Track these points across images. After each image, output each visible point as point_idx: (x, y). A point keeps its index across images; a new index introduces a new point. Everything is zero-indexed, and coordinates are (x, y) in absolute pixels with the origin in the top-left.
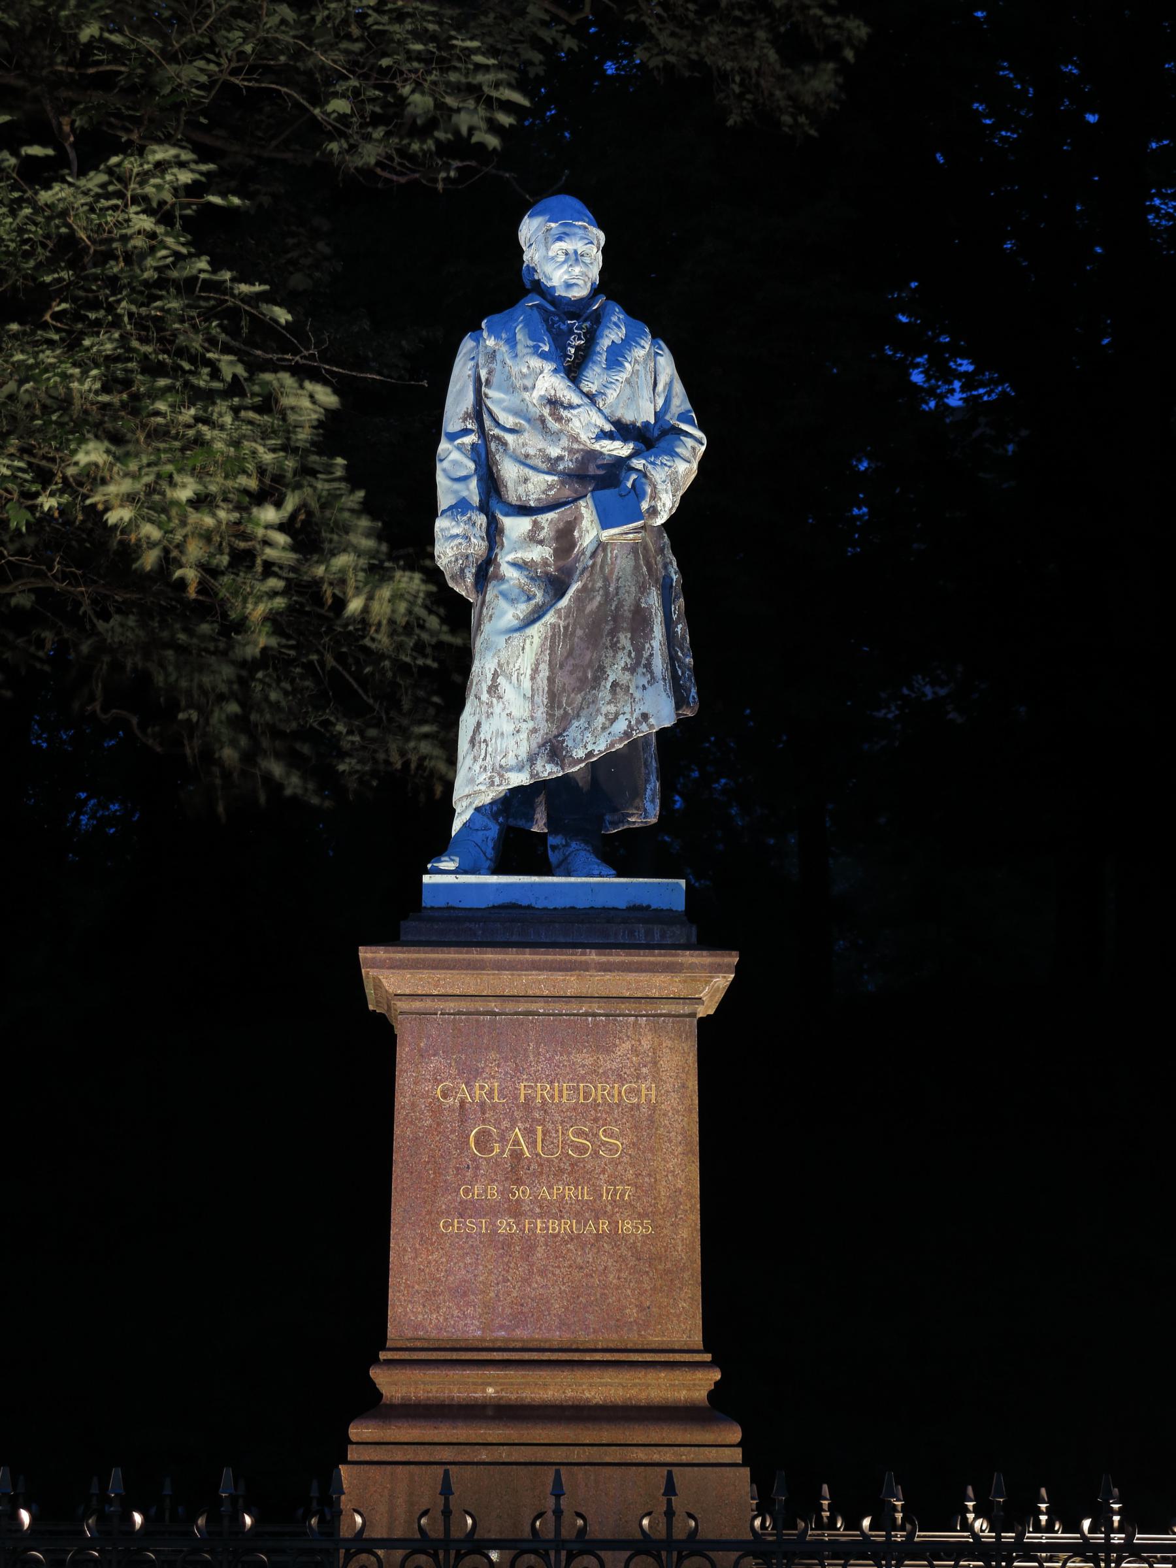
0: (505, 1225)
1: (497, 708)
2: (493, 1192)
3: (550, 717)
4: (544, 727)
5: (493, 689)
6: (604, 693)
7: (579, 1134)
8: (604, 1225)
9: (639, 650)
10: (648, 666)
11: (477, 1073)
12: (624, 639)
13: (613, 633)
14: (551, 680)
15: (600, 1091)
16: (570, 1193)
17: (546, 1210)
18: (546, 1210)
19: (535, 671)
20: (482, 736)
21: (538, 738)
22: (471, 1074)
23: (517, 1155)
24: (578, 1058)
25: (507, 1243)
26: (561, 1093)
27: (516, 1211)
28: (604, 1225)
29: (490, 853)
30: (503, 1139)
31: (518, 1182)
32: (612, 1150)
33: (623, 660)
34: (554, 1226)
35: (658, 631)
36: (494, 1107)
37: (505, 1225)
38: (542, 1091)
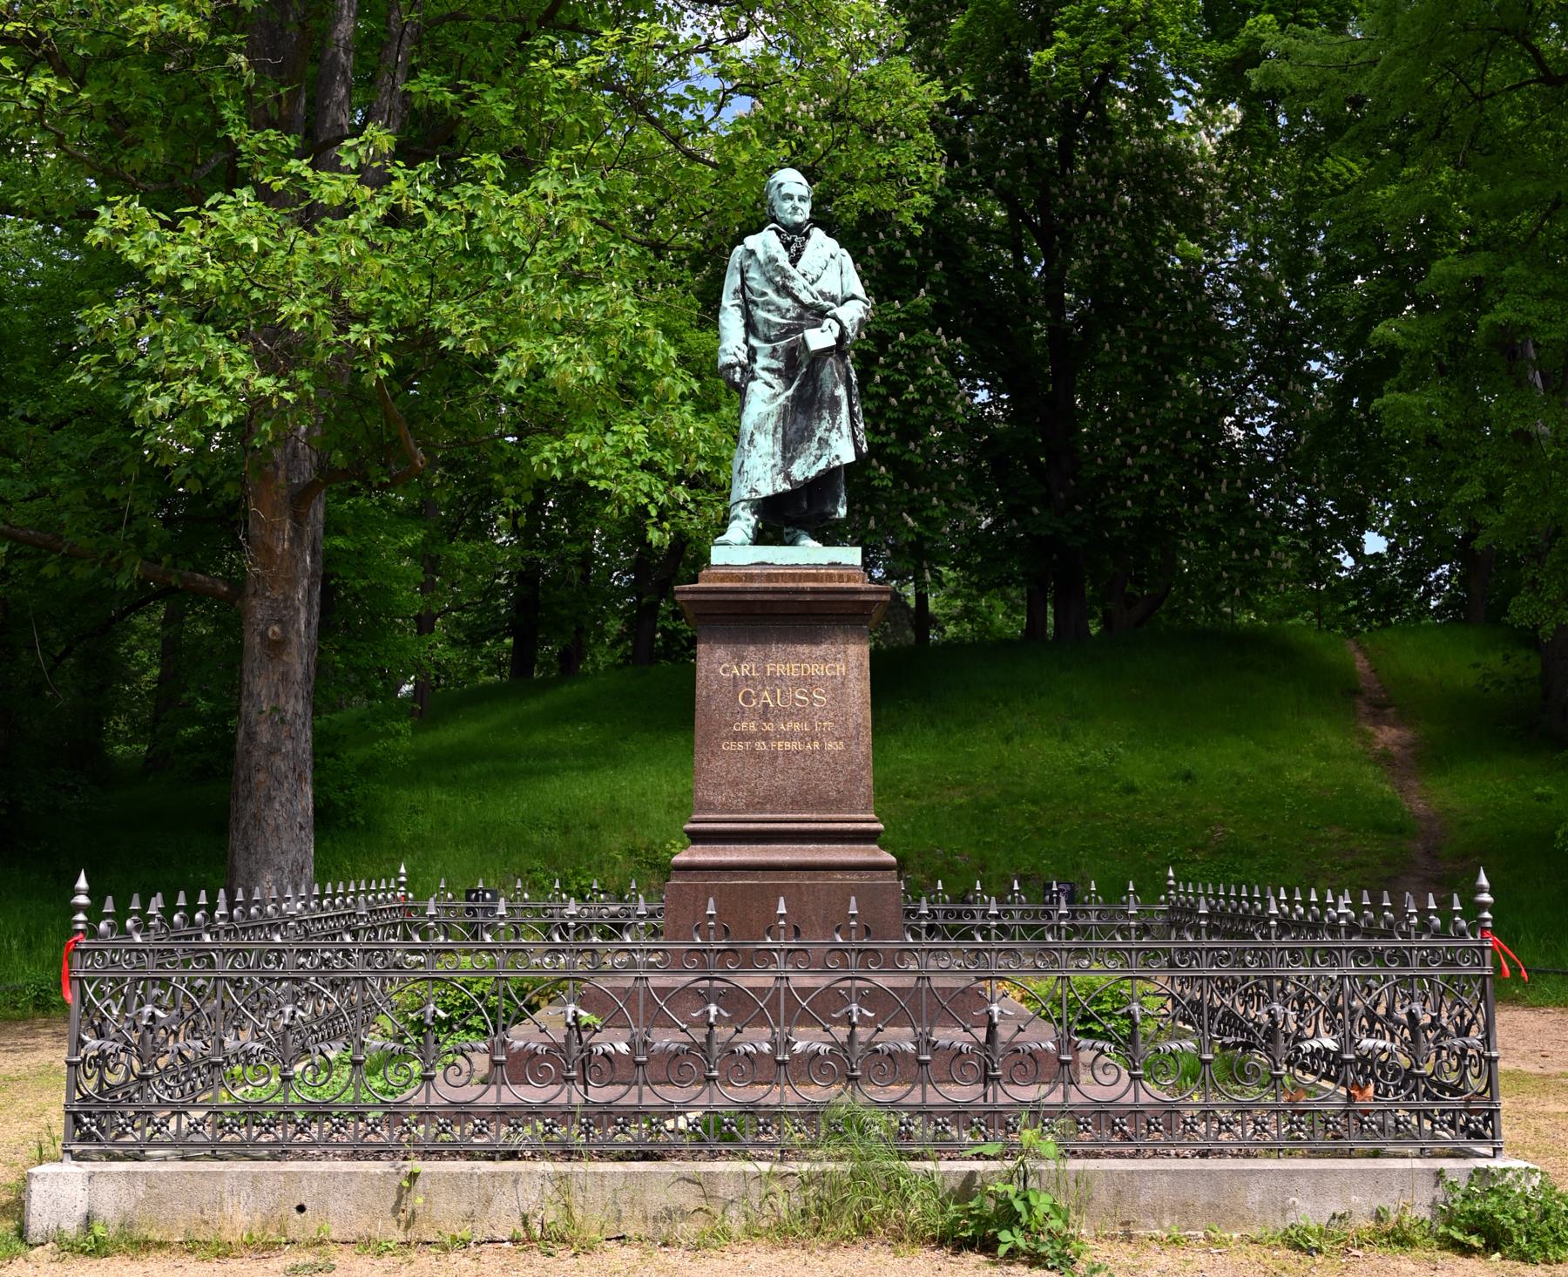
0: (760, 746)
1: (754, 452)
2: (753, 727)
3: (784, 458)
4: (780, 463)
5: (751, 442)
6: (815, 444)
7: (801, 693)
8: (816, 745)
9: (834, 419)
11: (742, 659)
12: (826, 414)
13: (819, 410)
15: (815, 669)
16: (797, 726)
17: (785, 737)
18: (785, 737)
19: (775, 431)
20: (745, 468)
21: (776, 470)
23: (766, 705)
25: (760, 756)
27: (766, 737)
28: (816, 745)
30: (758, 696)
31: (767, 720)
33: (825, 424)
34: (788, 745)
36: (753, 678)
37: (760, 746)
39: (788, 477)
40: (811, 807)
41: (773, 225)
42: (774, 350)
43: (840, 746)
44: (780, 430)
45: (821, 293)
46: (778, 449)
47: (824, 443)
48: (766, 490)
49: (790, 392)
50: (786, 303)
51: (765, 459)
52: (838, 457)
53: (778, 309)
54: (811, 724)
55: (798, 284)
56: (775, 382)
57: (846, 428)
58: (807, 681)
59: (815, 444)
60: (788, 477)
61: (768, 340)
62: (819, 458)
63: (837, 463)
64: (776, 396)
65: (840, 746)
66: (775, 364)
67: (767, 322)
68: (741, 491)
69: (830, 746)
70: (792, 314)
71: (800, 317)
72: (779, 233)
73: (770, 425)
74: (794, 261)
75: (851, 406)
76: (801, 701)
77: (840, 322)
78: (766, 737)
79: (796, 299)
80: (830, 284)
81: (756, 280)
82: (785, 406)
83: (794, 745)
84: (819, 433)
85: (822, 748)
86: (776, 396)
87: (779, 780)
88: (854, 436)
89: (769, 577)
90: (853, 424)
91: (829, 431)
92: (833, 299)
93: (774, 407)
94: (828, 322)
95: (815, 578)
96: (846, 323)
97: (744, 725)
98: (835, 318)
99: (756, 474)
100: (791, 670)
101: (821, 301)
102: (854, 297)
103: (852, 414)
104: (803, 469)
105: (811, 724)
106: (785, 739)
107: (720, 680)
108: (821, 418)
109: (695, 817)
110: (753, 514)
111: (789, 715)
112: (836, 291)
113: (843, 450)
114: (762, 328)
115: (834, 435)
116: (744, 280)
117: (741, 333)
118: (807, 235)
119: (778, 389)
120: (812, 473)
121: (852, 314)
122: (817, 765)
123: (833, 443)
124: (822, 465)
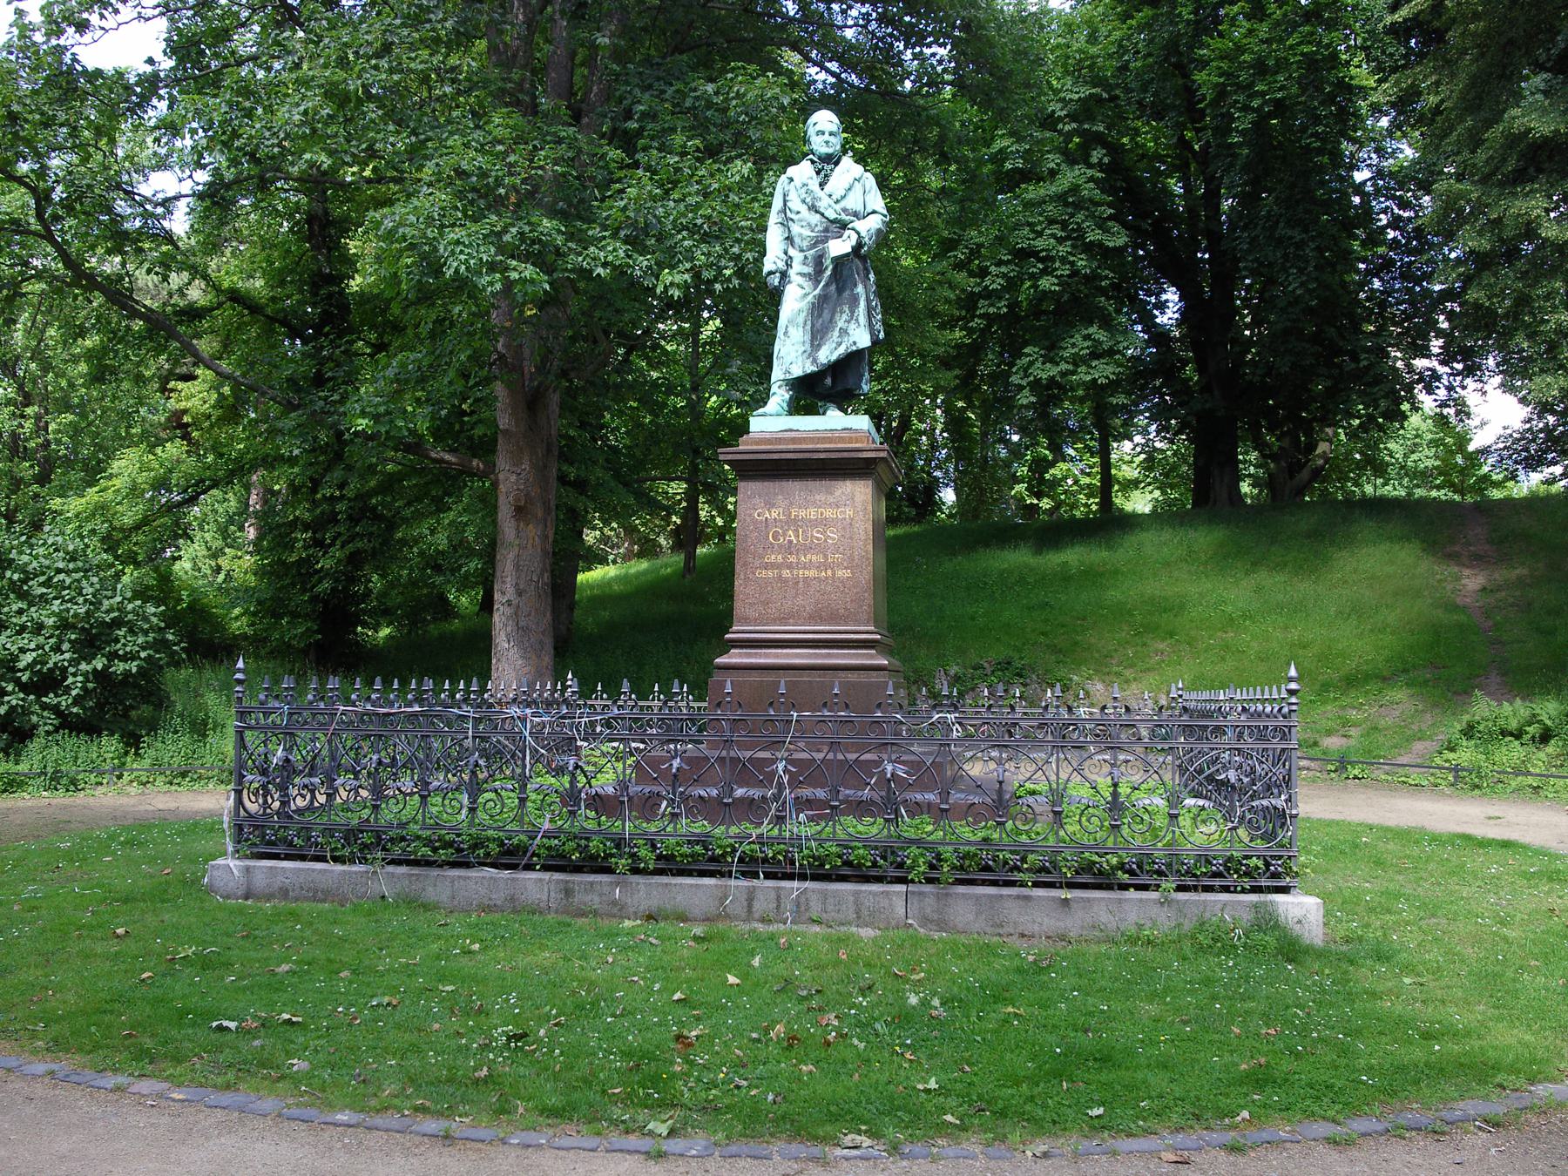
0: (786, 573)
3: (812, 345)
4: (809, 349)
5: (786, 333)
6: (836, 333)
7: (818, 532)
8: (829, 572)
9: (852, 312)
10: (857, 320)
11: (773, 506)
12: (846, 309)
14: (813, 326)
15: (828, 513)
16: (814, 558)
21: (806, 355)
22: (770, 505)
24: (817, 497)
25: (786, 581)
26: (812, 513)
27: (790, 567)
28: (829, 572)
29: (785, 405)
30: (784, 535)
32: (833, 539)
33: (845, 317)
34: (807, 572)
35: (862, 304)
37: (786, 573)
38: (802, 513)
39: (815, 361)
40: (822, 621)
41: (811, 156)
42: (806, 257)
43: (848, 573)
44: (809, 323)
45: (844, 210)
46: (808, 337)
47: (844, 332)
48: (797, 372)
49: (817, 292)
50: (815, 218)
51: (796, 347)
52: (855, 343)
53: (809, 224)
54: (826, 557)
55: (823, 205)
56: (805, 284)
57: (863, 319)
58: (824, 523)
59: (836, 333)
60: (815, 361)
61: (802, 251)
62: (839, 344)
63: (854, 348)
64: (806, 295)
65: (848, 573)
66: (807, 270)
67: (800, 235)
68: (777, 374)
69: (839, 573)
70: (819, 228)
71: (826, 230)
72: (813, 162)
73: (801, 319)
74: (822, 185)
75: (868, 301)
76: (818, 539)
77: (858, 233)
78: (790, 567)
79: (822, 215)
80: (854, 202)
81: (795, 204)
82: (813, 304)
83: (812, 573)
84: (841, 324)
85: (834, 575)
86: (806, 295)
87: (800, 601)
88: (871, 326)
89: (794, 440)
90: (870, 316)
91: (849, 322)
92: (856, 214)
93: (804, 305)
94: (847, 233)
95: (830, 440)
96: (863, 234)
97: (773, 557)
98: (853, 229)
99: (788, 360)
100: (812, 513)
101: (844, 217)
102: (874, 212)
103: (869, 309)
104: (829, 353)
105: (826, 557)
106: (805, 568)
107: (755, 522)
108: (842, 312)
109: (735, 628)
110: (788, 391)
111: (807, 549)
112: (860, 208)
113: (861, 338)
114: (797, 240)
115: (852, 326)
116: (785, 202)
117: (782, 246)
118: (837, 163)
119: (807, 290)
120: (834, 357)
121: (869, 226)
122: (829, 588)
123: (851, 332)
124: (841, 350)
